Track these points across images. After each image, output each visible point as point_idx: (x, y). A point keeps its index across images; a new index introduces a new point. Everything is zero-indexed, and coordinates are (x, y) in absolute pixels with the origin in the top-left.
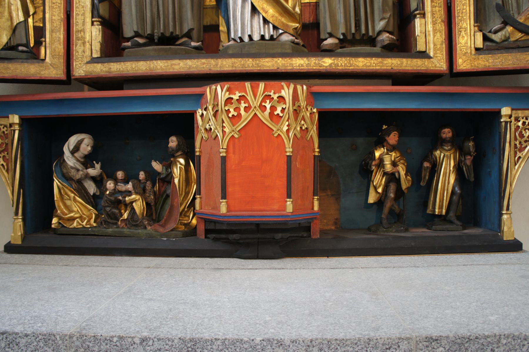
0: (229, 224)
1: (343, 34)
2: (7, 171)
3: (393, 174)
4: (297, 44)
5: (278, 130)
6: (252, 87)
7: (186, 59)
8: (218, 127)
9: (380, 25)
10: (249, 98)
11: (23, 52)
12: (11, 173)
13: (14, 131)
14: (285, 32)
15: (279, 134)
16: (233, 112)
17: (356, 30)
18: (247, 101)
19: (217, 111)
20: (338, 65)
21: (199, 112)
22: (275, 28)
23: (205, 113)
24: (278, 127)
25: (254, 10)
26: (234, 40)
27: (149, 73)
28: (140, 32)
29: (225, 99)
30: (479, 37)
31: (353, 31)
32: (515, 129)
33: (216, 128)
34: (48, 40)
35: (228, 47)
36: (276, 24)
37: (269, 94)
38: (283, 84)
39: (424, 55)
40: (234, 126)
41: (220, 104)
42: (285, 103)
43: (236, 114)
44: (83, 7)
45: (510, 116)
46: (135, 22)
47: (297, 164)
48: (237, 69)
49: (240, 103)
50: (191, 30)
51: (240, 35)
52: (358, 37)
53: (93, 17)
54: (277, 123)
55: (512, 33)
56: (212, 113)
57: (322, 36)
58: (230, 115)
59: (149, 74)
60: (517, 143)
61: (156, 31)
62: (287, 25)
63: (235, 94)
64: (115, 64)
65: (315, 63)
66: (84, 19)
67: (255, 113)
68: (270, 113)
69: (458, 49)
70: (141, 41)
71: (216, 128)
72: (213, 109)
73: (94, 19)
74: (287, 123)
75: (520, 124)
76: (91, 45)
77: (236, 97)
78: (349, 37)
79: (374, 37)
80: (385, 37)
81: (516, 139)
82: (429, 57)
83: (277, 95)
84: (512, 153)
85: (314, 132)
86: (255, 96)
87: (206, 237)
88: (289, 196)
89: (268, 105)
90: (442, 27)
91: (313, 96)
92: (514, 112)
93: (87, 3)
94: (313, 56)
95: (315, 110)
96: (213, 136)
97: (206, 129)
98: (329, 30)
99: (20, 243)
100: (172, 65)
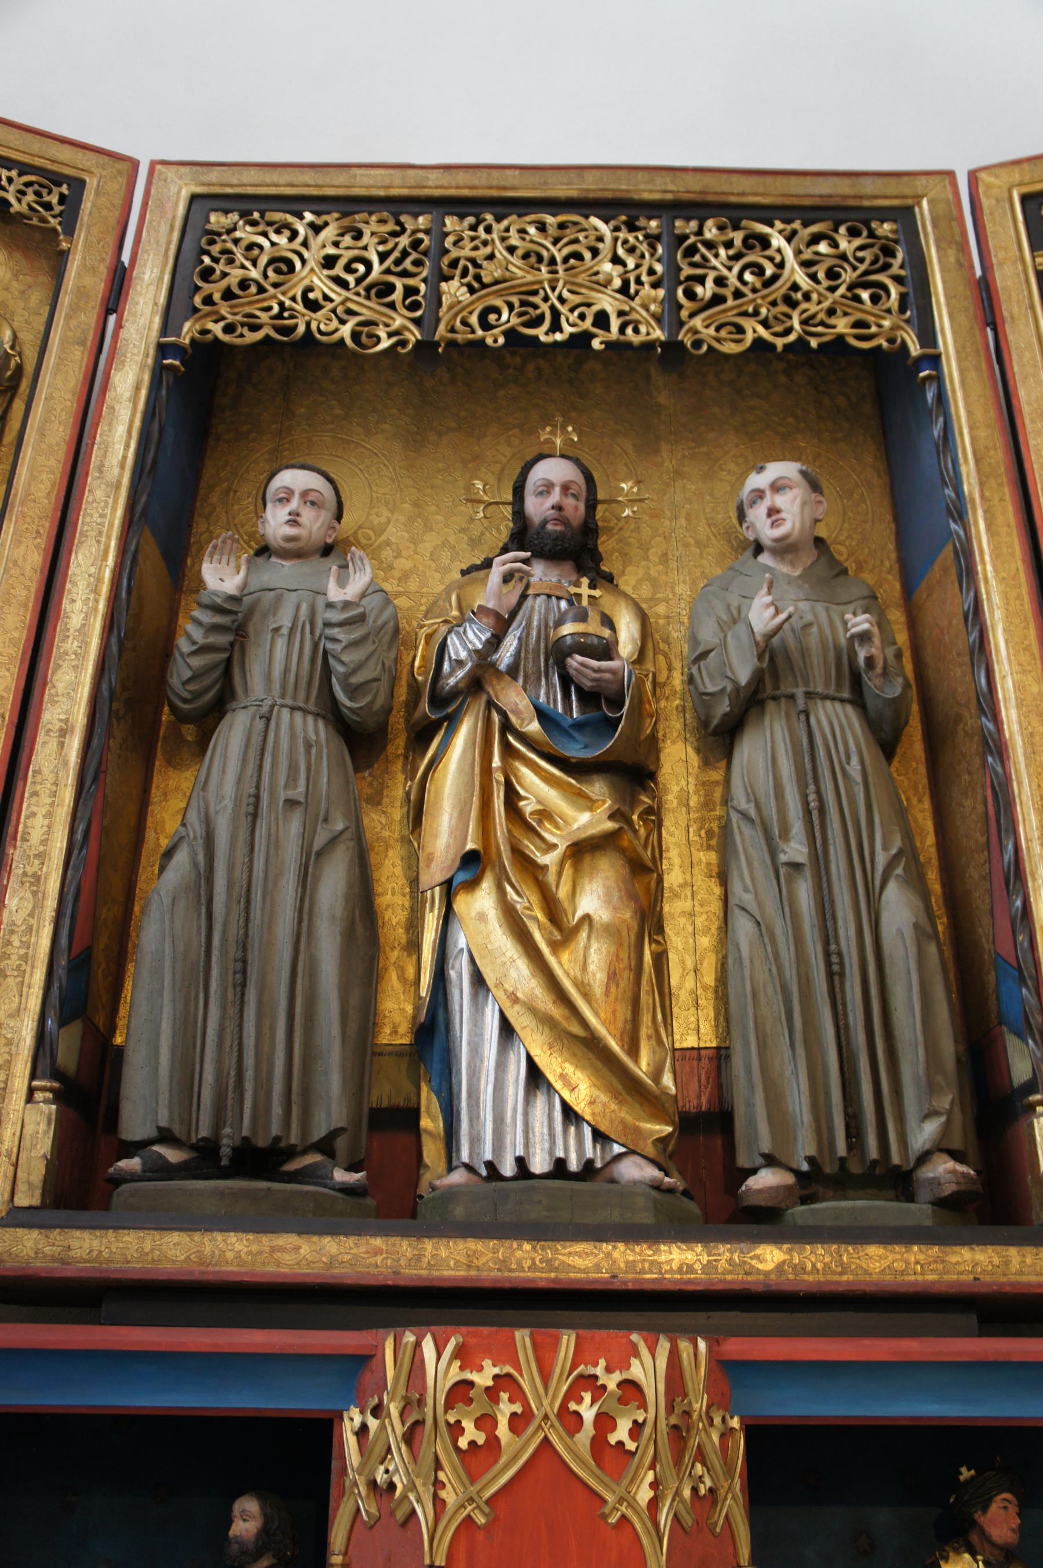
1: (810, 1160)
4: (670, 1191)
5: (621, 1500)
7: (322, 1233)
8: (418, 1482)
14: (631, 1152)
15: (623, 1517)
16: (471, 1433)
17: (850, 1147)
18: (518, 1394)
19: (419, 1423)
20: (804, 1269)
21: (353, 1420)
22: (599, 1136)
23: (373, 1423)
24: (621, 1491)
25: (535, 1076)
26: (469, 1168)
27: (196, 1272)
28: (178, 1130)
29: (449, 1384)
31: (841, 1149)
35: (451, 1194)
36: (603, 1128)
37: (591, 1371)
38: (635, 1337)
40: (473, 1480)
41: (430, 1402)
42: (643, 1406)
43: (481, 1438)
44: (9, 1042)
46: (164, 1098)
48: (484, 1274)
50: (334, 1134)
51: (488, 1156)
52: (855, 1168)
53: (33, 1076)
54: (617, 1475)
56: (399, 1430)
57: (743, 1161)
58: (463, 1443)
59: (197, 1277)
61: (227, 1130)
62: (637, 1131)
63: (480, 1369)
64: (86, 1234)
65: (730, 1261)
66: (7, 1079)
68: (594, 1439)
70: (173, 1155)
71: (412, 1487)
72: (402, 1414)
73: (35, 1083)
74: (650, 1476)
76: (16, 1166)
77: (483, 1379)
78: (828, 1169)
79: (906, 1168)
83: (617, 1377)
86: (546, 1376)
89: (588, 1412)
93: (24, 1032)
94: (725, 1239)
95: (735, 1423)
96: (400, 1514)
97: (373, 1484)
98: (766, 1145)
100: (273, 1250)
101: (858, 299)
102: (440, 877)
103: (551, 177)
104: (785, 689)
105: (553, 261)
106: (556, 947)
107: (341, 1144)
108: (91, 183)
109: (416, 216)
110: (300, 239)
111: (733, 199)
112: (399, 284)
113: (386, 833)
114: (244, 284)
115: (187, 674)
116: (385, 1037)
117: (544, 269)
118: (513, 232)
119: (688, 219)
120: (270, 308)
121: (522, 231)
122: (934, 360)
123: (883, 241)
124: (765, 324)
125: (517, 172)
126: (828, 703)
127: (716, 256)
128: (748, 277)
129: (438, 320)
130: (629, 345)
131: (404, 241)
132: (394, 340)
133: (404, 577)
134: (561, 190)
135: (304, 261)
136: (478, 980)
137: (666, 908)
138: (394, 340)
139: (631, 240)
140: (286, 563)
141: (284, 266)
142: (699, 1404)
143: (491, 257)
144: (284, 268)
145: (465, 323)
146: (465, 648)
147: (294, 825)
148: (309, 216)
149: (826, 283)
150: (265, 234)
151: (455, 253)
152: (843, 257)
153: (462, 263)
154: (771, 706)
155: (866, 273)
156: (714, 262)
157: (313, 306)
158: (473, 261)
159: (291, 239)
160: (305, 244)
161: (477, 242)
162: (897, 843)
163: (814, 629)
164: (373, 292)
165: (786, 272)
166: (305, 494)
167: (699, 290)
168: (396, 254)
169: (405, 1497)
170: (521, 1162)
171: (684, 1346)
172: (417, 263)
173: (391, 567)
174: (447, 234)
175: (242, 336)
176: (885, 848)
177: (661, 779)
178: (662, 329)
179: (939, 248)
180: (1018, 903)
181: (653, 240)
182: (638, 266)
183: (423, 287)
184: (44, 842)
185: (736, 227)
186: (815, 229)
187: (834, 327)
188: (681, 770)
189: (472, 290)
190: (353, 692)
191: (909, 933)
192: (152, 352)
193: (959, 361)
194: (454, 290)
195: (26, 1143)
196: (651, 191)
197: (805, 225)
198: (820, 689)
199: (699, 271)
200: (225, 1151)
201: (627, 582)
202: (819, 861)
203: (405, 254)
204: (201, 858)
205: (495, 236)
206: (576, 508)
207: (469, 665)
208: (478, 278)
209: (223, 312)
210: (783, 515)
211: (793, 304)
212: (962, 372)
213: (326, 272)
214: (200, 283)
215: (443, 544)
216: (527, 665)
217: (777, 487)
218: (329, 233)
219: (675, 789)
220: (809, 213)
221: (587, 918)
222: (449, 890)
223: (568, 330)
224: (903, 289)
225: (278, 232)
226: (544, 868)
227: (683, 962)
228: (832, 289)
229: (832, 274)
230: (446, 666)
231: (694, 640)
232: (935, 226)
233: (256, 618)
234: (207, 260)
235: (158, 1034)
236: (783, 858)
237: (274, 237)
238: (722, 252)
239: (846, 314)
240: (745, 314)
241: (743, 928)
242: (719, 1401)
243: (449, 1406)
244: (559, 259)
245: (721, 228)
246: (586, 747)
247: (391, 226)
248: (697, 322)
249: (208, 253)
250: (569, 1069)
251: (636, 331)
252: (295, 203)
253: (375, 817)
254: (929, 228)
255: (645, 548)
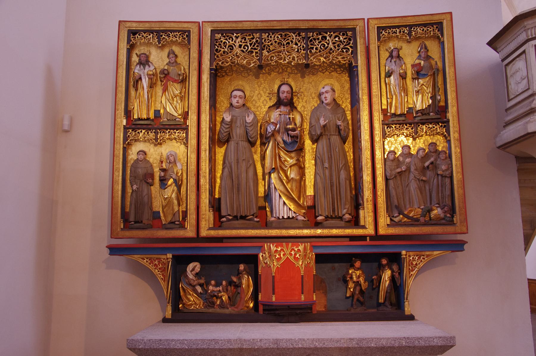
0: (276, 306)
2: (164, 281)
3: (358, 282)
4: (305, 221)
6: (286, 245)
9: (345, 211)
10: (285, 250)
11: (177, 224)
12: (166, 282)
13: (169, 261)
16: (278, 256)
17: (333, 213)
18: (284, 251)
21: (261, 254)
22: (294, 212)
23: (264, 255)
24: (297, 263)
25: (284, 203)
26: (275, 217)
28: (231, 215)
30: (388, 219)
31: (331, 214)
32: (409, 261)
33: (270, 263)
34: (188, 219)
35: (272, 222)
39: (364, 227)
42: (301, 252)
43: (279, 257)
45: (406, 255)
47: (305, 279)
49: (281, 252)
50: (254, 214)
51: (278, 216)
52: (334, 216)
53: (209, 208)
55: (402, 219)
57: (317, 215)
58: (277, 257)
60: (410, 267)
63: (279, 248)
65: (313, 232)
67: (288, 257)
69: (380, 225)
70: (230, 218)
71: (270, 263)
75: (411, 258)
77: (279, 249)
78: (330, 216)
79: (341, 216)
80: (347, 216)
81: (409, 266)
82: (366, 228)
83: (297, 249)
84: (408, 272)
85: (313, 263)
86: (287, 249)
87: (263, 313)
88: (302, 293)
89: (293, 253)
90: (372, 214)
91: (313, 247)
92: (408, 253)
95: (314, 254)
96: (268, 266)
97: (264, 263)
99: (171, 317)
101: (343, 52)
102: (268, 171)
103: (284, 23)
104: (327, 133)
105: (284, 45)
106: (287, 183)
107: (255, 215)
108: (191, 30)
109: (256, 33)
110: (234, 41)
111: (319, 27)
112: (254, 51)
113: (257, 159)
114: (224, 52)
115: (223, 136)
116: (260, 195)
117: (282, 47)
118: (276, 38)
119: (310, 32)
120: (230, 58)
121: (278, 37)
122: (357, 67)
123: (349, 37)
124: (325, 58)
125: (276, 22)
126: (334, 136)
127: (316, 42)
128: (322, 48)
129: (262, 59)
130: (299, 64)
131: (254, 40)
132: (254, 64)
133: (257, 108)
134: (285, 27)
135: (235, 46)
136: (275, 188)
137: (306, 171)
138: (254, 64)
139: (299, 39)
140: (237, 109)
141: (231, 47)
142: (308, 252)
143: (272, 44)
144: (232, 48)
145: (267, 59)
146: (271, 130)
147: (244, 164)
148: (235, 34)
149: (337, 48)
150: (226, 39)
151: (265, 43)
152: (341, 41)
153: (266, 46)
154: (324, 136)
155: (346, 45)
156: (316, 44)
157: (238, 57)
158: (268, 45)
159: (232, 41)
160: (235, 42)
161: (269, 41)
162: (344, 162)
163: (332, 122)
164: (249, 53)
165: (330, 46)
166: (239, 96)
167: (312, 51)
168: (253, 44)
169: (269, 264)
170: (283, 217)
171: (306, 244)
172: (257, 46)
173: (255, 105)
174: (263, 39)
175: (225, 64)
176: (341, 164)
177: (305, 147)
178: (305, 60)
179: (360, 39)
180: (361, 175)
181: (303, 38)
182: (301, 45)
183: (259, 52)
184: (205, 170)
185: (320, 34)
186: (336, 34)
187: (338, 58)
188: (308, 145)
189: (268, 52)
190: (252, 138)
191: (344, 180)
192: (209, 70)
193: (361, 67)
194: (265, 52)
195: (210, 218)
196: (303, 26)
197: (334, 33)
198: (333, 133)
199: (312, 46)
200: (239, 217)
201: (299, 108)
202: (330, 166)
203: (255, 44)
204: (230, 170)
205: (272, 39)
206: (289, 96)
207: (271, 133)
208: (269, 49)
209: (221, 59)
210: (327, 98)
211: (330, 53)
212: (361, 70)
213: (240, 49)
214: (216, 53)
215: (264, 100)
216: (281, 131)
217: (327, 92)
218: (239, 39)
219: (307, 149)
220: (335, 30)
221: (292, 178)
222: (270, 174)
223: (287, 61)
224: (352, 50)
225: (229, 39)
226: (286, 170)
227: (308, 180)
228: (338, 49)
229: (338, 46)
230: (267, 133)
231: (310, 123)
232: (360, 33)
233: (233, 123)
234: (216, 47)
235: (227, 200)
236: (324, 166)
237: (228, 40)
238: (317, 41)
239: (341, 55)
240: (321, 56)
241: (318, 177)
242: (311, 251)
243: (275, 253)
244: (285, 44)
245: (317, 34)
246: (292, 148)
247: (252, 37)
248: (312, 58)
249: (216, 45)
250: (290, 202)
251: (300, 61)
252: (232, 31)
253: (255, 156)
254: (358, 34)
255: (302, 99)
